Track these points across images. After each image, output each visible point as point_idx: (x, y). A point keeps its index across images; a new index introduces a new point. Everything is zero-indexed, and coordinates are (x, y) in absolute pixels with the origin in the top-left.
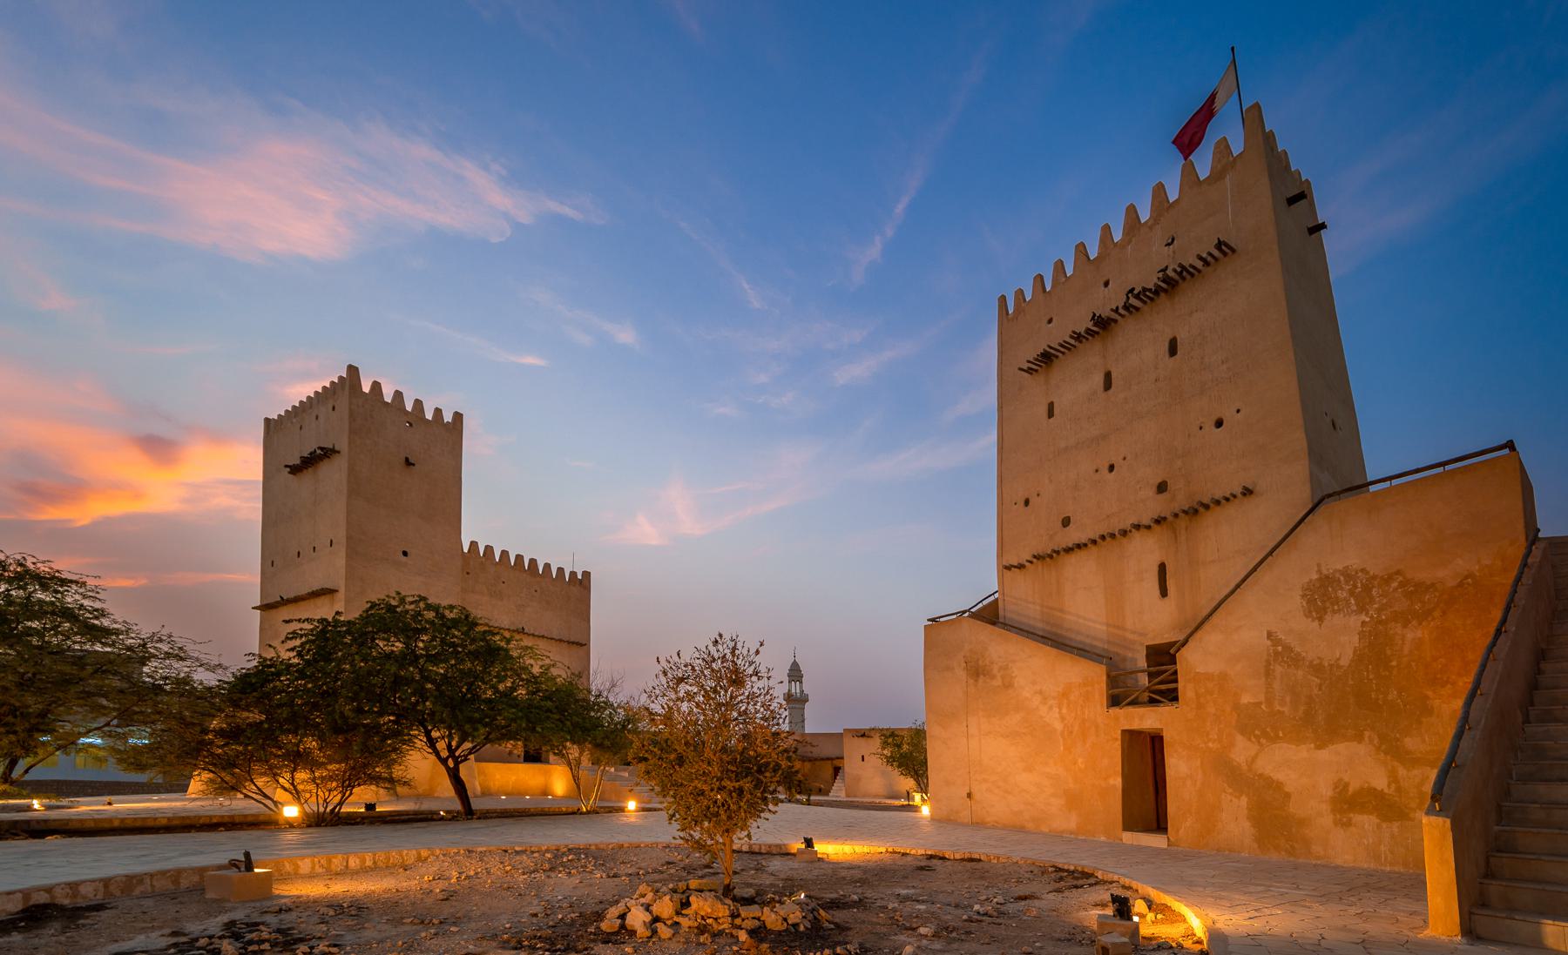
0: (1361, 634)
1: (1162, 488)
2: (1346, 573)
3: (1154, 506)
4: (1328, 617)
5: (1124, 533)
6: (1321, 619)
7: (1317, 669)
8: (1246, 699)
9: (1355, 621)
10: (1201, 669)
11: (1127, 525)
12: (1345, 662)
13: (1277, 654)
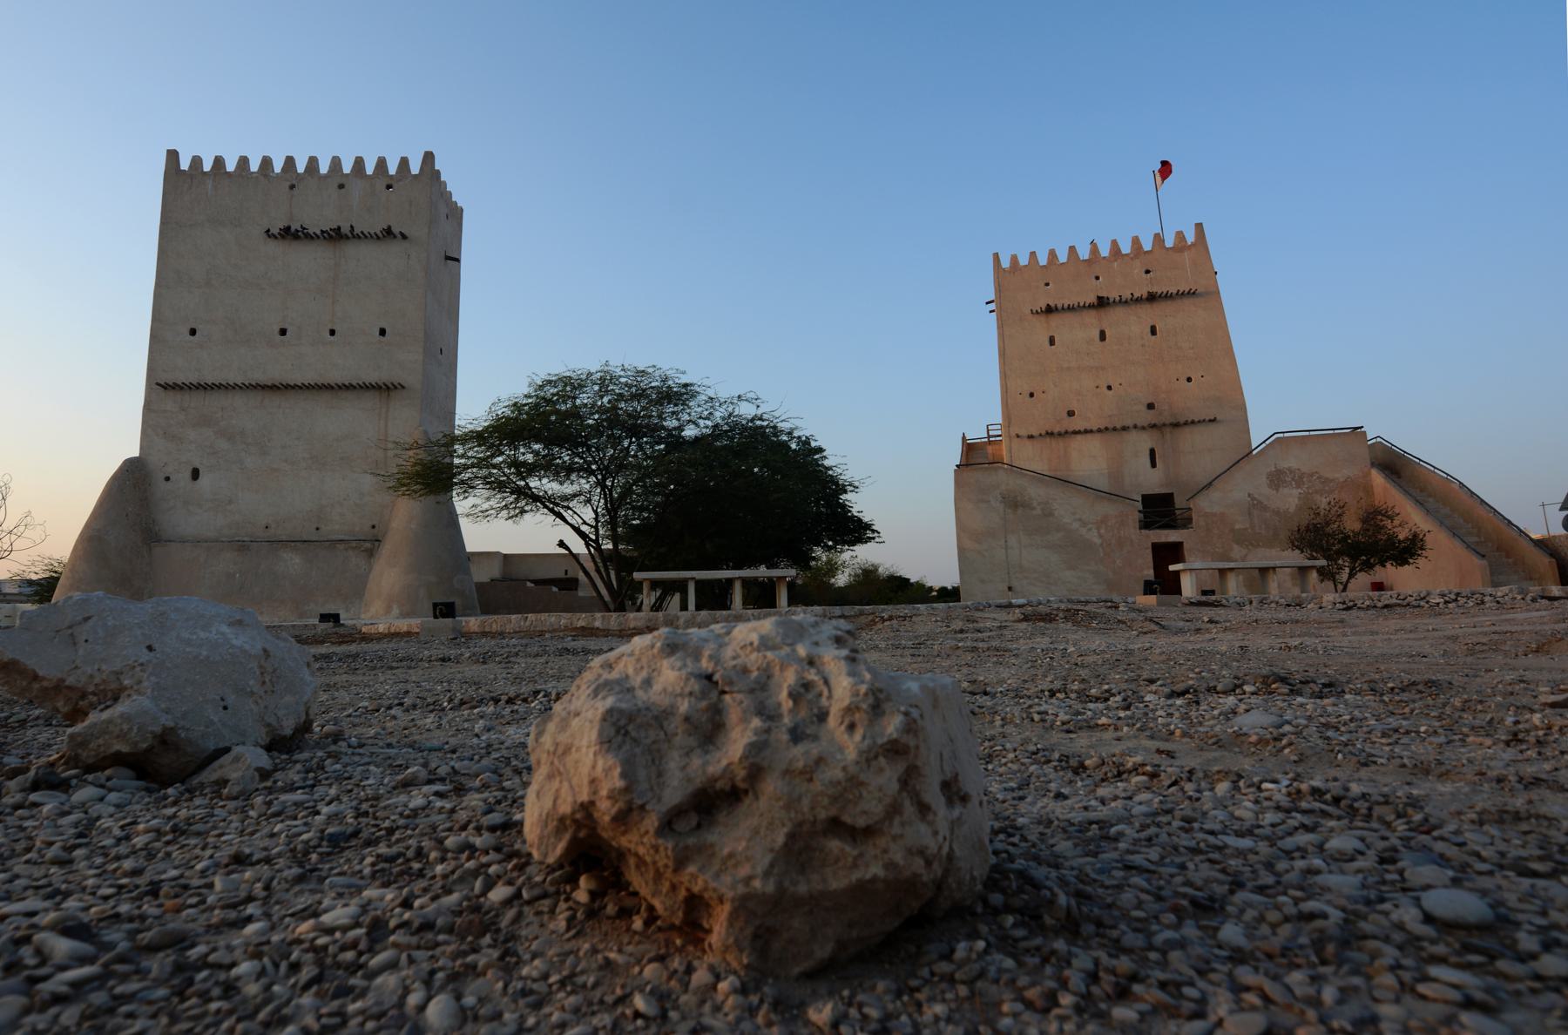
0: (1299, 498)
1: (1151, 406)
2: (1290, 469)
3: (1147, 417)
4: (1281, 489)
5: (1124, 429)
6: (1277, 490)
7: (1277, 513)
8: (1237, 527)
9: (1296, 492)
10: (1208, 510)
11: (1129, 423)
12: (1291, 510)
13: (1254, 505)
